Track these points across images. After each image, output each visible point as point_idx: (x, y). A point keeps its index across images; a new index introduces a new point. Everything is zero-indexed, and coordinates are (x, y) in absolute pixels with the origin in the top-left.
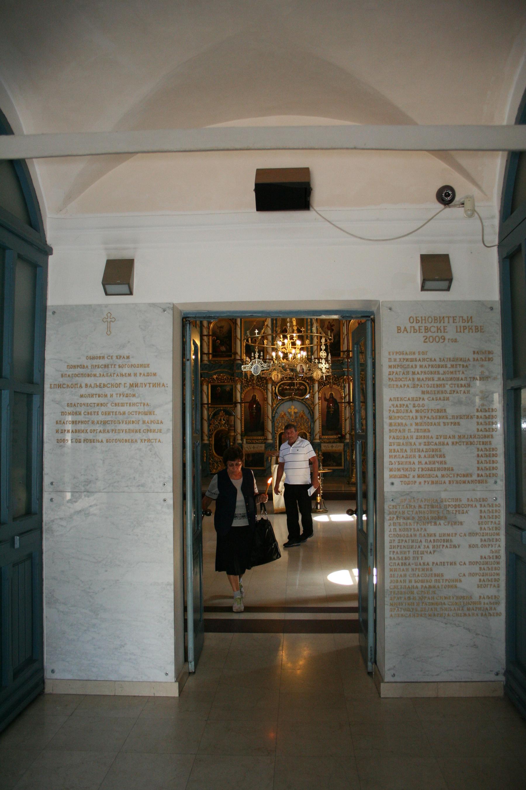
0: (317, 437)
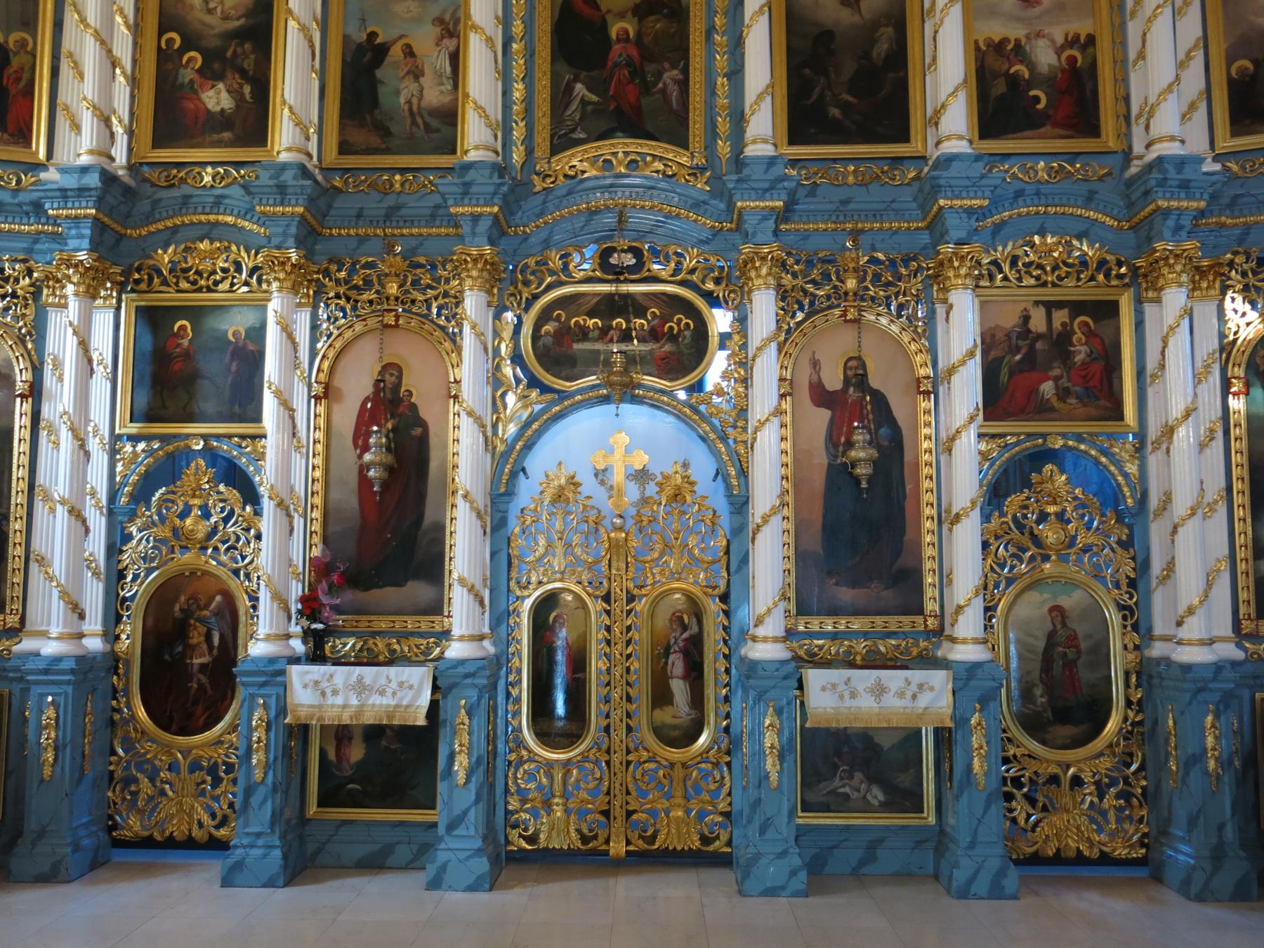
0: (774, 626)
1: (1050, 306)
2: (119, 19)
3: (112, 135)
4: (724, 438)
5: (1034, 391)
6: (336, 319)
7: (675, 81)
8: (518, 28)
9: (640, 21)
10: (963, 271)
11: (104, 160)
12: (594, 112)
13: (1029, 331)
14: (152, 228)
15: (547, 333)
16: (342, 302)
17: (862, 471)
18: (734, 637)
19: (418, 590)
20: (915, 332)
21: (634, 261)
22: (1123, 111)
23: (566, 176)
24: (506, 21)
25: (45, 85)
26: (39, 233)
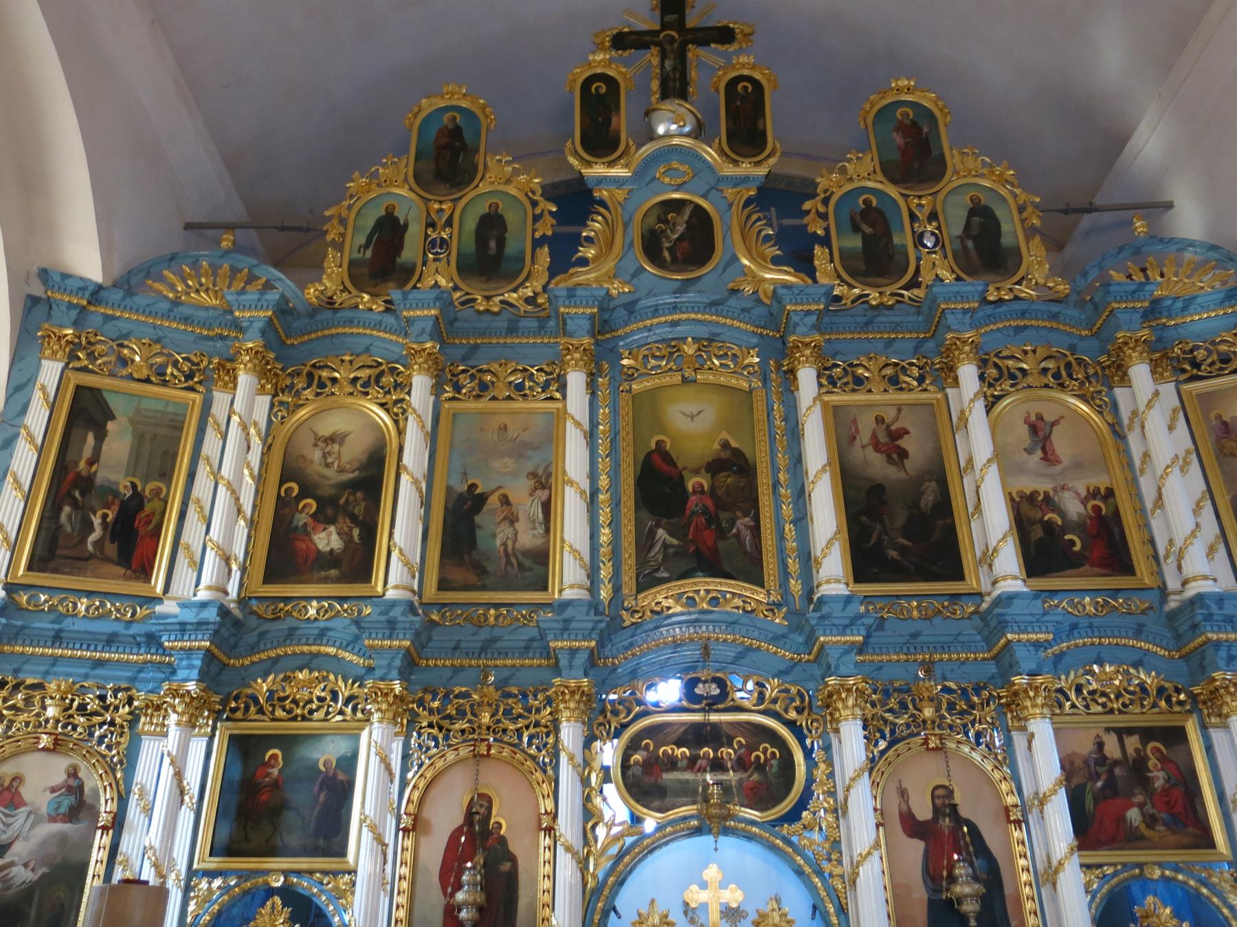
1: (1121, 733)
2: (246, 472)
3: (230, 570)
4: (819, 873)
5: (1121, 819)
6: (428, 748)
7: (747, 527)
8: (604, 481)
9: (712, 477)
10: (1039, 701)
11: (220, 594)
12: (676, 554)
13: (1105, 758)
14: (256, 658)
15: (636, 763)
16: (435, 731)
17: (970, 907)
20: (996, 758)
21: (718, 691)
22: (1151, 552)
23: (652, 611)
24: (593, 476)
25: (172, 527)
26: (146, 662)
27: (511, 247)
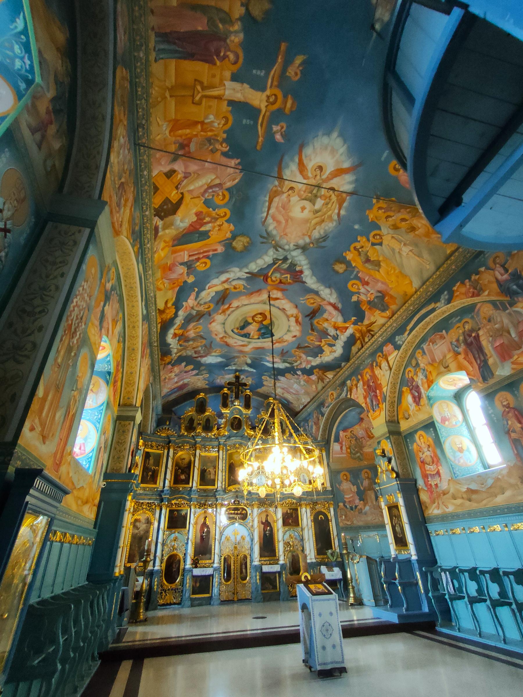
0: (258, 559)
8: (224, 468)
18: (251, 561)
19: (208, 556)
27: (211, 425)
